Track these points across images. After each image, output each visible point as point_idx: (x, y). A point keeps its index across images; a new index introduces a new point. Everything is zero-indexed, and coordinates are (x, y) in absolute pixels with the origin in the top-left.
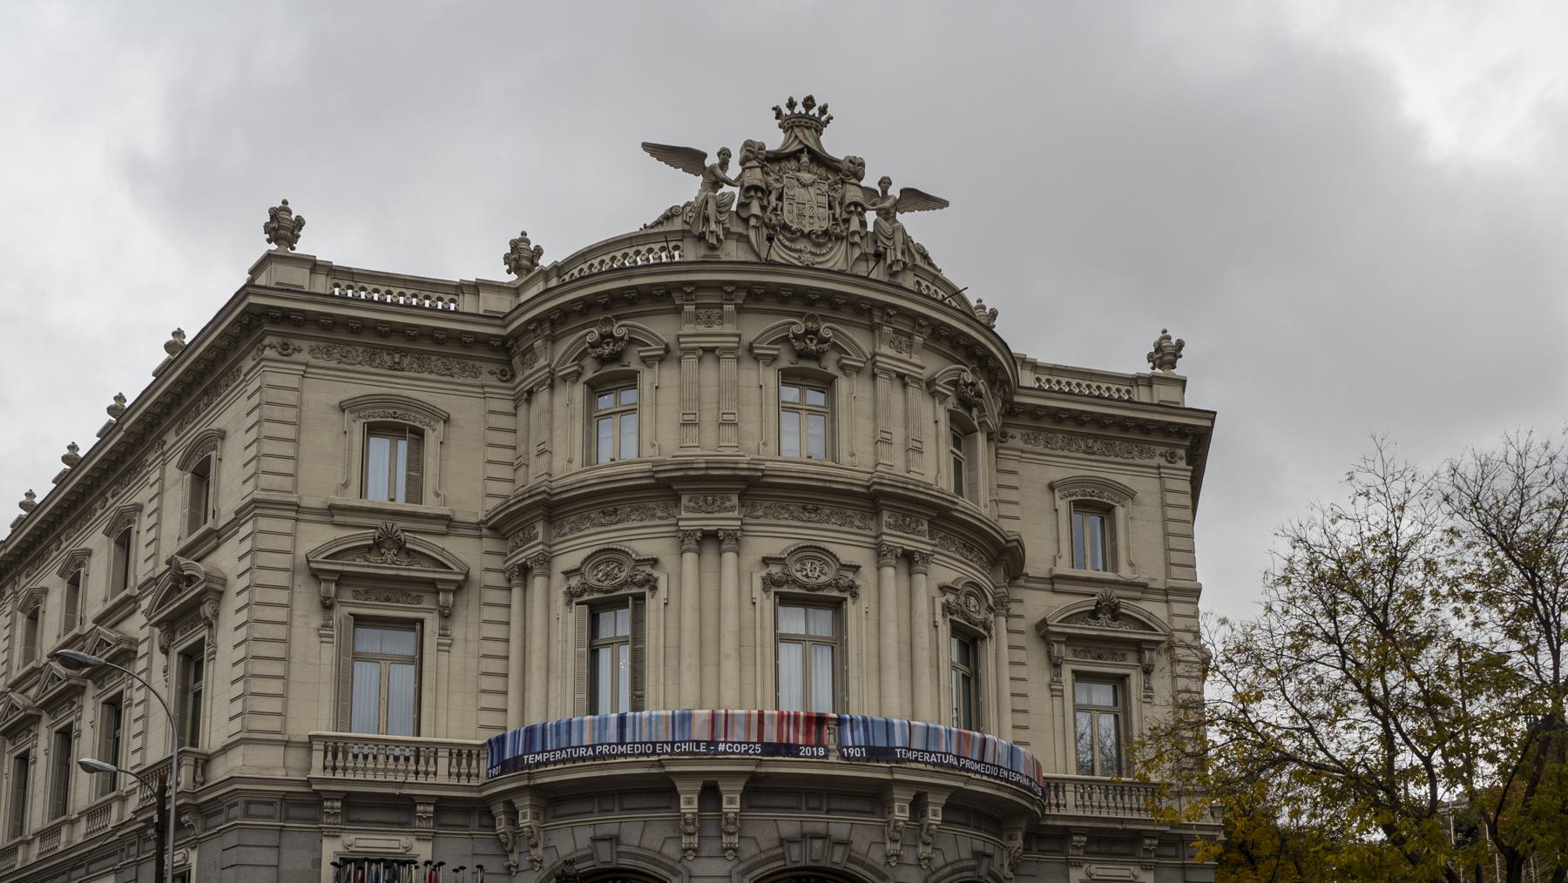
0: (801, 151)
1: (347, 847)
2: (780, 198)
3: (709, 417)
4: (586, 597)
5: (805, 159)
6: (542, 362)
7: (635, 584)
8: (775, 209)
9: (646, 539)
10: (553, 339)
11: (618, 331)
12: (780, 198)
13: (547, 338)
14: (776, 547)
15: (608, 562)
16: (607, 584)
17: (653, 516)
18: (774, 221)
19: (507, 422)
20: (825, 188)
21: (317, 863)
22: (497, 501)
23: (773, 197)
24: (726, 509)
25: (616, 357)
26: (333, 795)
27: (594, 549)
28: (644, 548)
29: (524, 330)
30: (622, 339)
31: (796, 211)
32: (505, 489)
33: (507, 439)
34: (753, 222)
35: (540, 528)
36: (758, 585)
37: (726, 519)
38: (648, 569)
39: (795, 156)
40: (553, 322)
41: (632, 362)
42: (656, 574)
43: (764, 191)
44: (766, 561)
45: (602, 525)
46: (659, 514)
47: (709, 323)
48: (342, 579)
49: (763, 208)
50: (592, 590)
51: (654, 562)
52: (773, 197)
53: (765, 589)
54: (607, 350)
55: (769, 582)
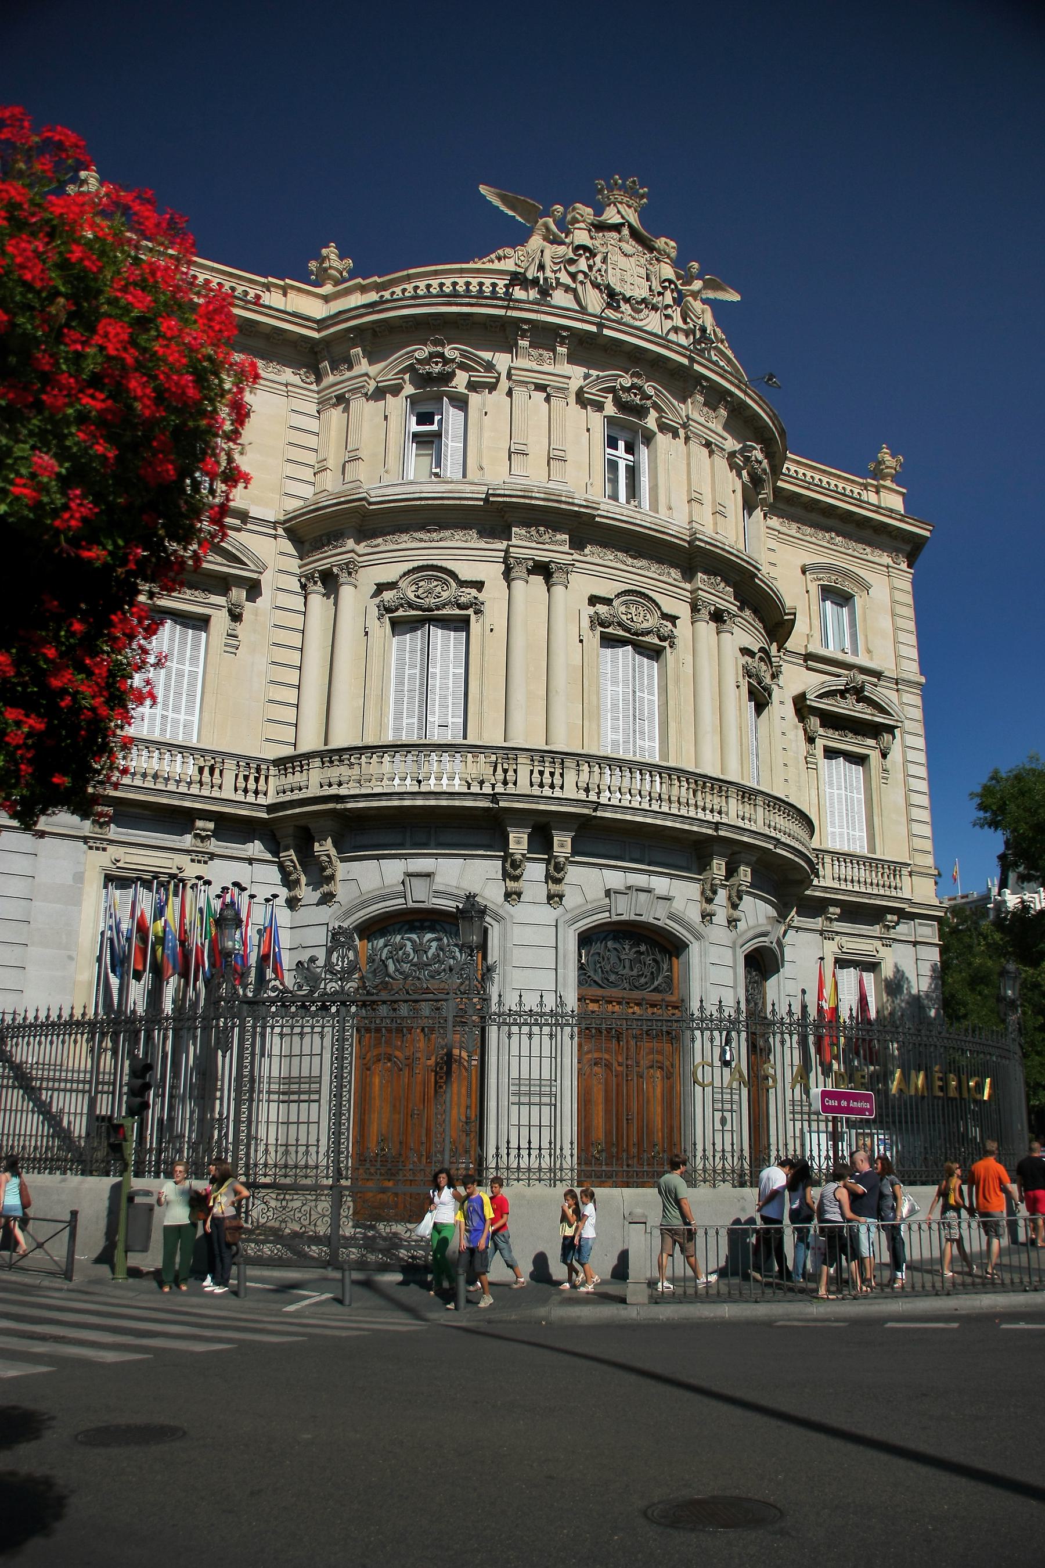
0: (623, 225)
2: (604, 261)
3: (538, 450)
5: (626, 231)
7: (461, 607)
8: (600, 270)
9: (473, 559)
11: (449, 352)
12: (604, 261)
14: (606, 589)
15: (430, 579)
16: (431, 601)
18: (599, 280)
19: (313, 425)
20: (643, 261)
22: (301, 503)
24: (555, 543)
27: (416, 564)
28: (466, 571)
30: (453, 360)
31: (619, 277)
32: (307, 491)
33: (312, 441)
34: (581, 277)
36: (586, 623)
38: (474, 592)
39: (617, 228)
42: (481, 597)
43: (591, 253)
44: (593, 600)
47: (540, 360)
49: (590, 268)
50: (411, 606)
51: (479, 585)
52: (598, 259)
53: (592, 628)
54: (437, 369)
55: (597, 621)
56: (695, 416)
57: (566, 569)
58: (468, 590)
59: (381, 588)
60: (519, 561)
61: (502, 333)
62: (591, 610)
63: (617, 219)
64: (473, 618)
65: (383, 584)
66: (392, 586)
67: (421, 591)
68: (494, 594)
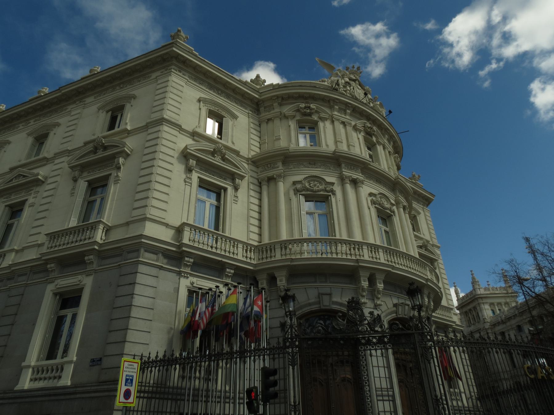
1: (192, 284)
2: (353, 88)
4: (303, 193)
6: (277, 110)
10: (281, 105)
11: (312, 106)
13: (279, 103)
16: (315, 188)
17: (330, 169)
21: (177, 290)
23: (352, 88)
25: (310, 115)
26: (190, 255)
29: (271, 98)
30: (314, 109)
35: (280, 164)
37: (357, 175)
40: (283, 99)
41: (315, 117)
44: (371, 194)
45: (309, 167)
46: (332, 168)
48: (199, 161)
50: (307, 190)
52: (352, 88)
56: (386, 141)
57: (362, 182)
58: (329, 186)
59: (294, 183)
60: (346, 177)
61: (329, 102)
62: (371, 198)
63: (354, 78)
64: (332, 196)
65: (296, 182)
66: (300, 182)
67: (311, 185)
68: (337, 189)
